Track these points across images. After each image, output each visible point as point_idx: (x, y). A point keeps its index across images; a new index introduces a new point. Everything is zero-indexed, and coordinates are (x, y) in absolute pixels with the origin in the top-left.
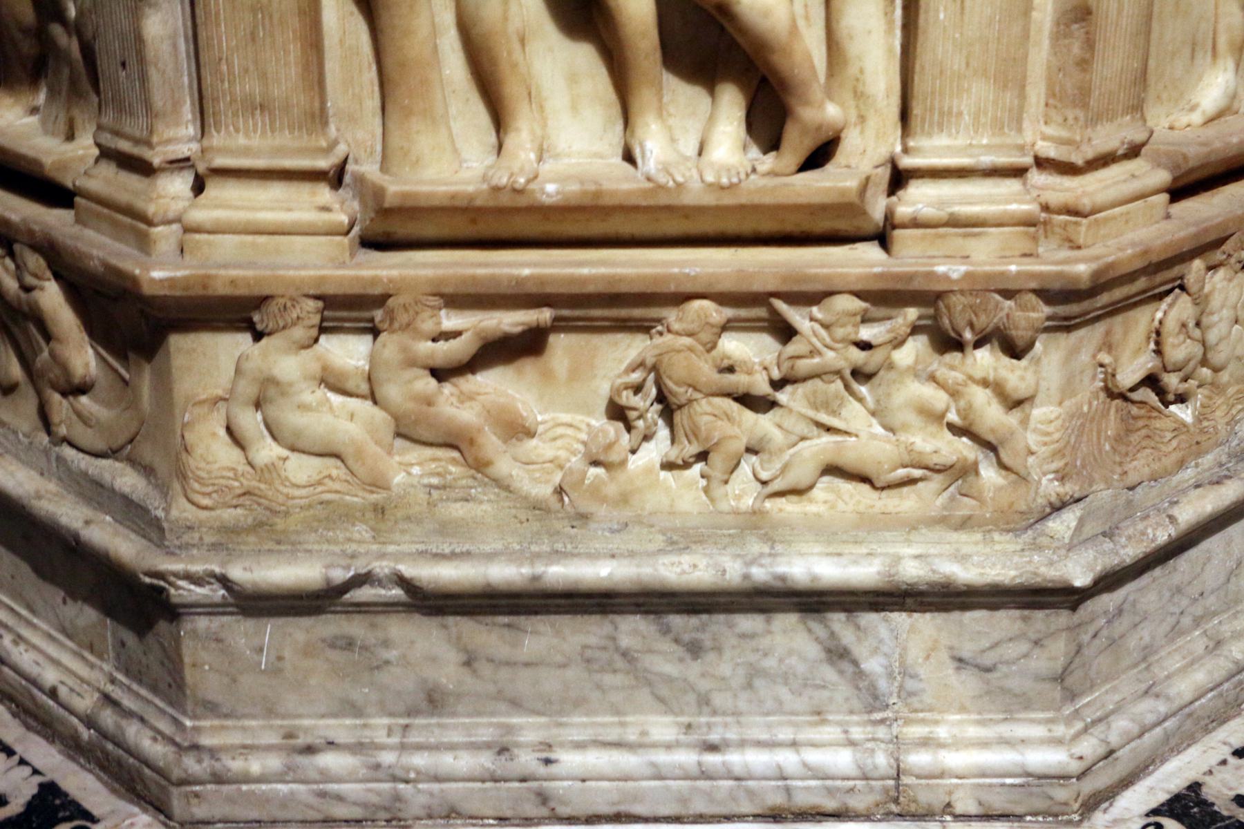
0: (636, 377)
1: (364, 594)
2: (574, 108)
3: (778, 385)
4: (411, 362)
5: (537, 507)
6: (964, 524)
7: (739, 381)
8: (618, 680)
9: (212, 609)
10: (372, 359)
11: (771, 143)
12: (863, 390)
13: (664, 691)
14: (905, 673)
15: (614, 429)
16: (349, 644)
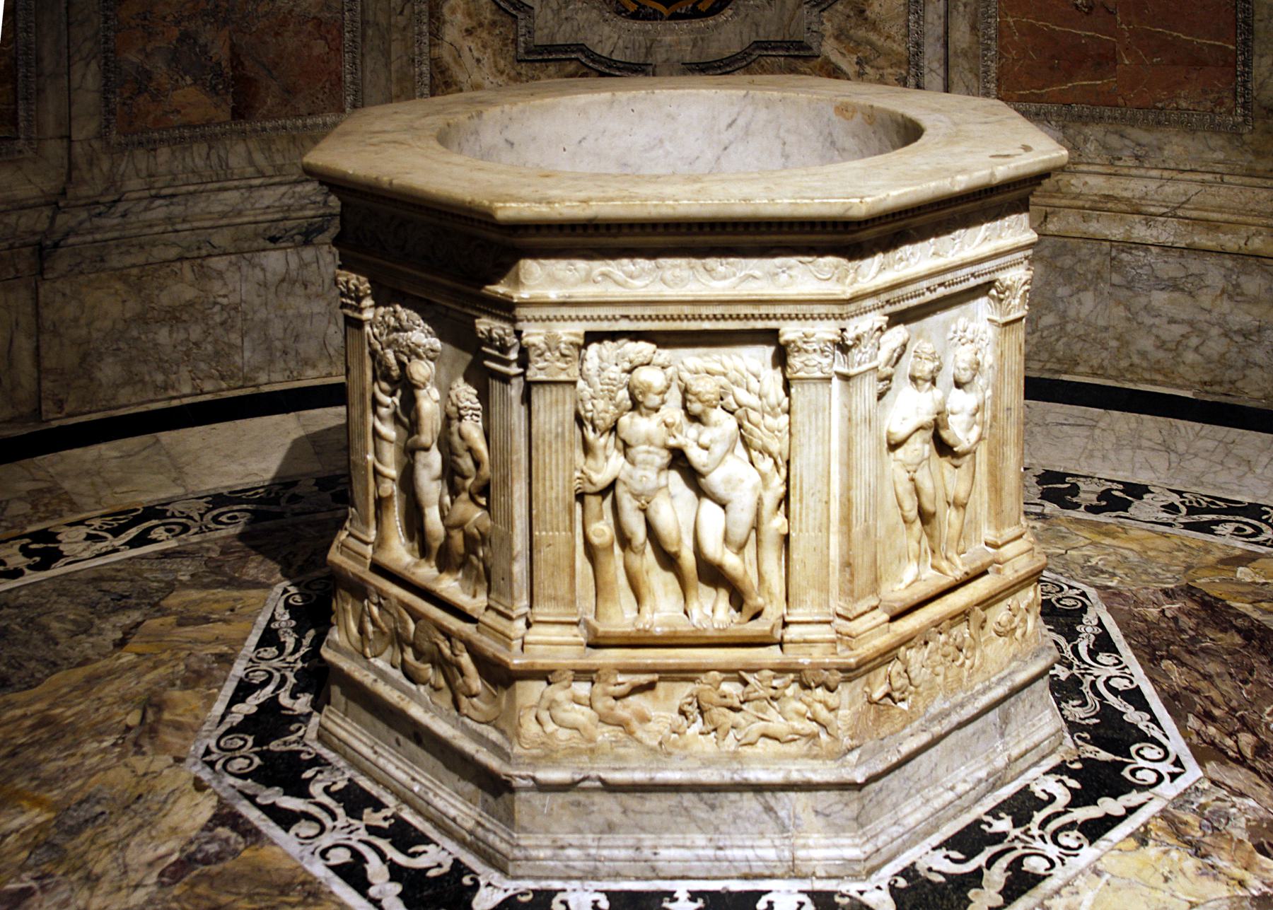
0: (689, 700)
1: (586, 784)
2: (666, 595)
3: (742, 703)
4: (606, 694)
5: (652, 749)
6: (815, 757)
7: (728, 701)
8: (683, 819)
9: (527, 789)
10: (592, 693)
11: (739, 610)
12: (775, 704)
13: (701, 824)
14: (795, 817)
15: (681, 719)
16: (579, 804)
